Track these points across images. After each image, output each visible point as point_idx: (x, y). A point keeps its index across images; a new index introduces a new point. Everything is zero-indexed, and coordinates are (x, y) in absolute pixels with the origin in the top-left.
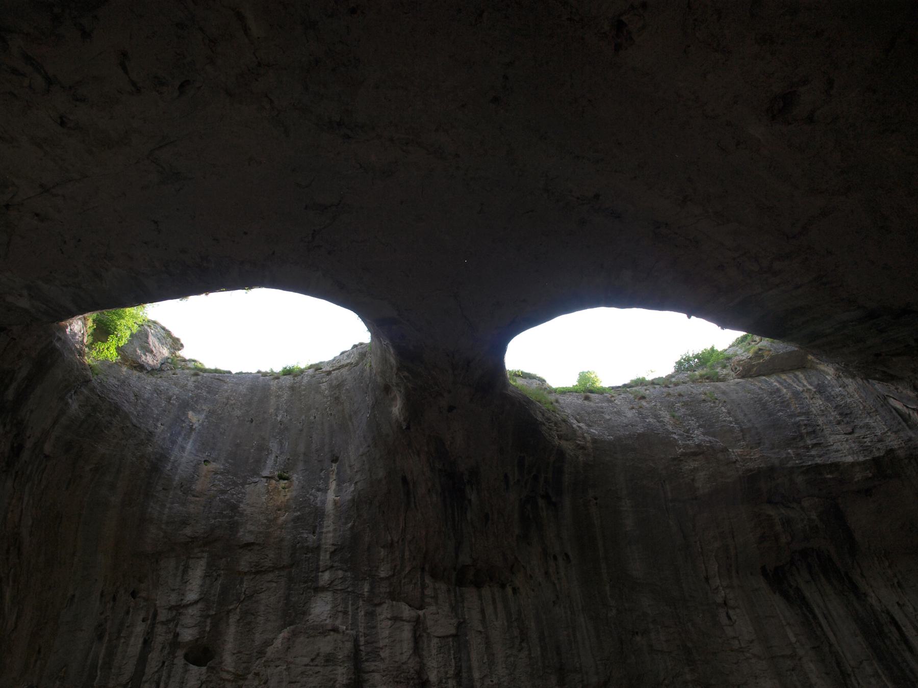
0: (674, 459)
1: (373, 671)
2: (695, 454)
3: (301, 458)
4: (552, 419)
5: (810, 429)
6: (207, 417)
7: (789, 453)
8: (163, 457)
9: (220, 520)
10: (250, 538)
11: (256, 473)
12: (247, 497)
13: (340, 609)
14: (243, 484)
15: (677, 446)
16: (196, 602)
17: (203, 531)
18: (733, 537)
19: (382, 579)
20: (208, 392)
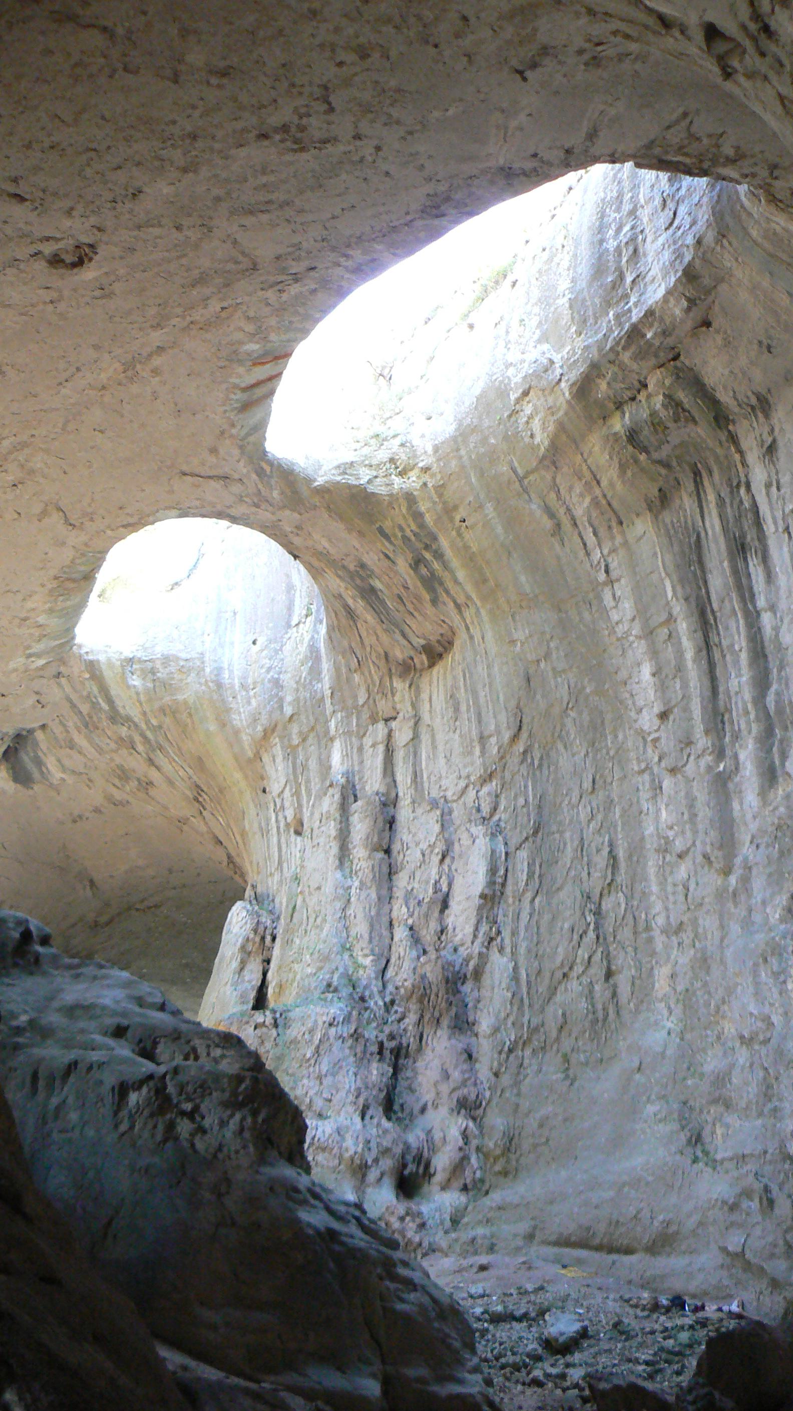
0: (510, 416)
2: (526, 393)
5: (631, 249)
8: (219, 670)
10: (288, 710)
11: (289, 626)
14: (281, 650)
18: (598, 483)
19: (363, 706)
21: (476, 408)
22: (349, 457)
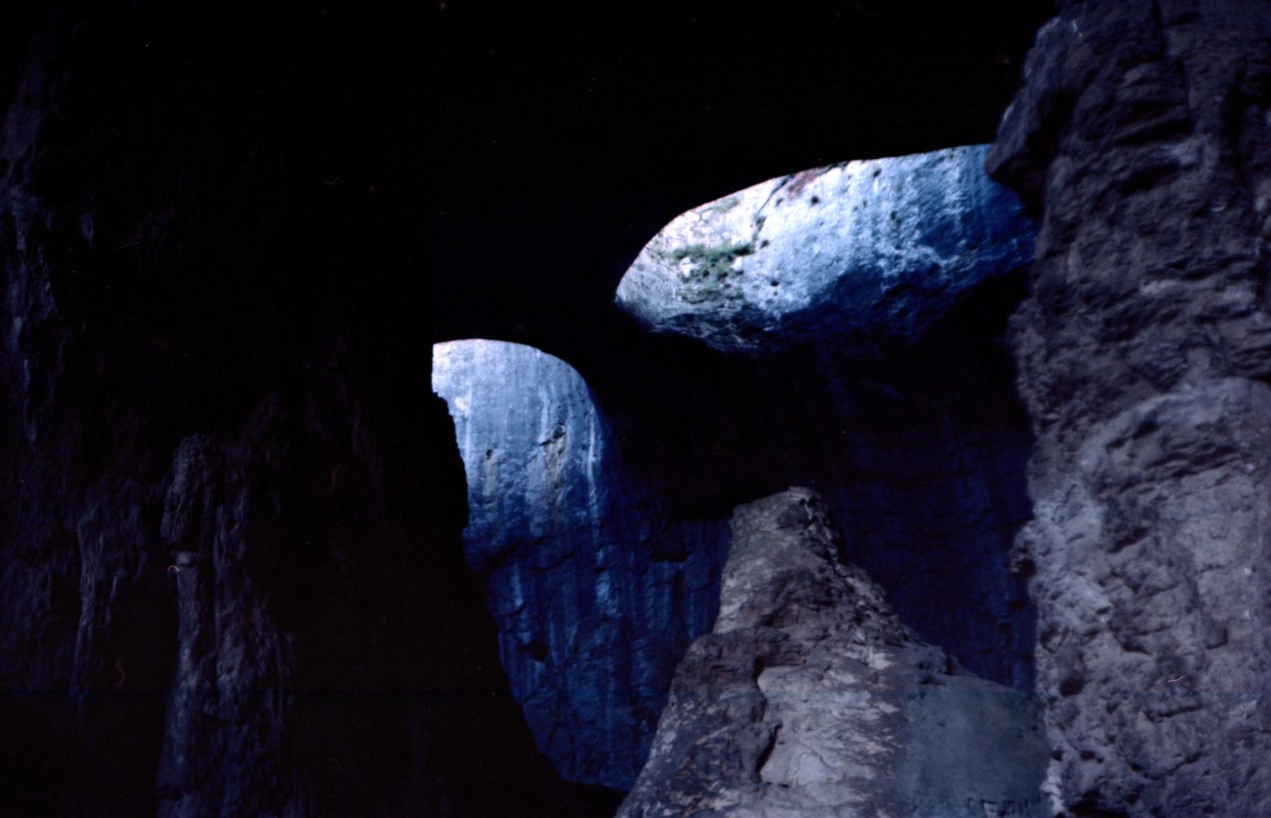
0: (877, 306)
1: (638, 649)
3: (569, 402)
4: (728, 318)
6: (474, 394)
7: (1012, 246)
9: (513, 521)
10: (538, 532)
11: (534, 444)
12: (531, 479)
13: (616, 586)
14: (524, 465)
15: (883, 280)
16: (522, 607)
17: (503, 539)
20: (466, 360)
21: (837, 287)
22: (690, 309)
